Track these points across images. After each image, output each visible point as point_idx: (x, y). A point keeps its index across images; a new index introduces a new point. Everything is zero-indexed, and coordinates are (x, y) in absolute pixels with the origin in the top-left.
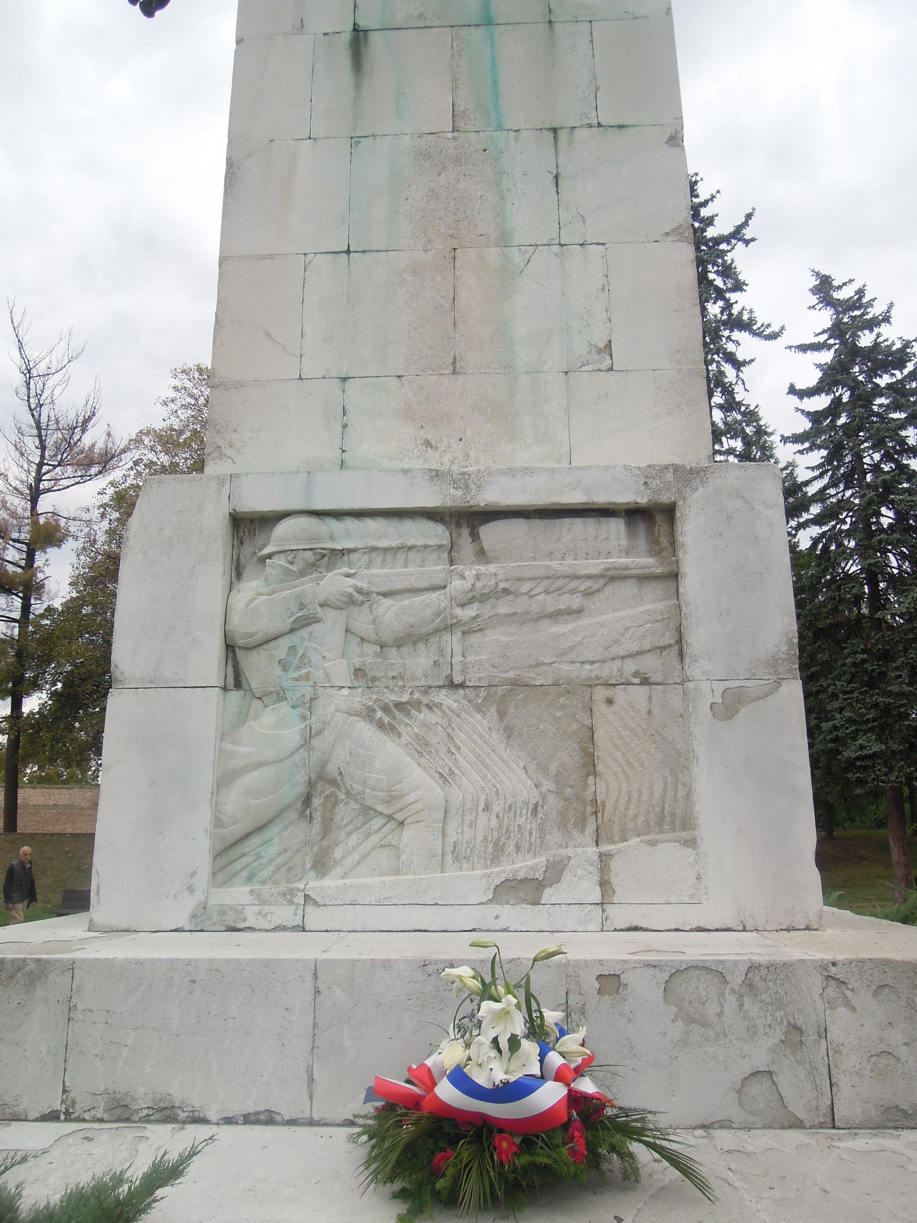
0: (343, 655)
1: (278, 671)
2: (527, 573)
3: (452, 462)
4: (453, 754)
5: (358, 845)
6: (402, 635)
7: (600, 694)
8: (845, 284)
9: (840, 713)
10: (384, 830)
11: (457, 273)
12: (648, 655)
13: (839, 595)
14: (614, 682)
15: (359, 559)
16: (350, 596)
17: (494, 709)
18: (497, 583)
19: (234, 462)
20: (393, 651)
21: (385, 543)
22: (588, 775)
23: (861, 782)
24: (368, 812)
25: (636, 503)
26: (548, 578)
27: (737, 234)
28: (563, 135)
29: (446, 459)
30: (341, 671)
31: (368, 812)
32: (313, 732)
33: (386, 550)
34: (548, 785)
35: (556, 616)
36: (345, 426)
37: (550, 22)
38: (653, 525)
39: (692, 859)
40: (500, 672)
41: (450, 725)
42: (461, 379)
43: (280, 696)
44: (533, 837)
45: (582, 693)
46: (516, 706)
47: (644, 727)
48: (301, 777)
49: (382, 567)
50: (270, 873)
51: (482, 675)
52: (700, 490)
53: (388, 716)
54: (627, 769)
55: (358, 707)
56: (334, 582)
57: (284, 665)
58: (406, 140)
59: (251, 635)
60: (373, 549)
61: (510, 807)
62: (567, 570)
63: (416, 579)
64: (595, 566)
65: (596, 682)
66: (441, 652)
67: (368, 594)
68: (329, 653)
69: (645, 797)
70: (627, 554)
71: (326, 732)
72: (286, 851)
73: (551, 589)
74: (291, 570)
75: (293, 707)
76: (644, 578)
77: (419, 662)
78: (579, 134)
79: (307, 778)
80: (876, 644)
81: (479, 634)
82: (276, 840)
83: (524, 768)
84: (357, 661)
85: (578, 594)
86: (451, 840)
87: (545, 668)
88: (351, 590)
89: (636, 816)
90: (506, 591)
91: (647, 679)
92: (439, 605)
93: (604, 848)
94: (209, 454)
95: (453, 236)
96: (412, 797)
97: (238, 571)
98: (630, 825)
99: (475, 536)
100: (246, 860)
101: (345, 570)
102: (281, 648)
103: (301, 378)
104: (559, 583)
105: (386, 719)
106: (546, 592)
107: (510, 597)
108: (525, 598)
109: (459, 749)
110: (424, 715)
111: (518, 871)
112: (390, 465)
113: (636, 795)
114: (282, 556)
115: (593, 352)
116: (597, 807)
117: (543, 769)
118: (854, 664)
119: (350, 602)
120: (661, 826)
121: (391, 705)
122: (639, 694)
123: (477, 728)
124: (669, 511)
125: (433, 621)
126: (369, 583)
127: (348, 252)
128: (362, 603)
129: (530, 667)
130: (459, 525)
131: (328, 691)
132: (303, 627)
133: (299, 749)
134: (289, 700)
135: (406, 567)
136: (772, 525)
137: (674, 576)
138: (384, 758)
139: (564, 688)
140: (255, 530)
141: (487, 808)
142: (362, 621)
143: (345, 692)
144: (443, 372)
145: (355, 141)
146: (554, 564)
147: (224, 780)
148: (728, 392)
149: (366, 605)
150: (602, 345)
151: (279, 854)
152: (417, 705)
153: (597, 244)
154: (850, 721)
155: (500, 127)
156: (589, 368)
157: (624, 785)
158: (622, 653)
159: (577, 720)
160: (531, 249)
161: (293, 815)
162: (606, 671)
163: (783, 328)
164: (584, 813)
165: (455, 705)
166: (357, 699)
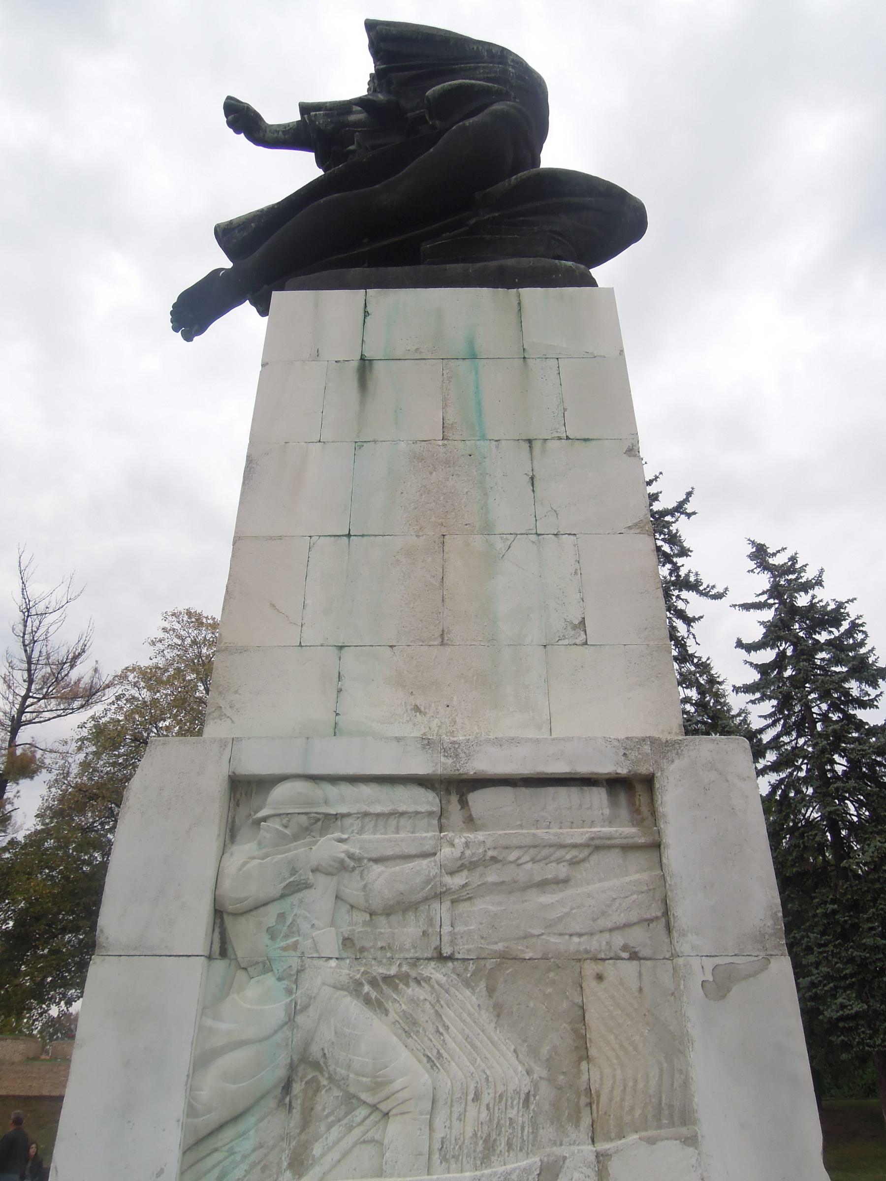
0: (333, 924)
1: (266, 940)
2: (515, 842)
3: (440, 727)
4: (441, 1034)
5: (339, 1140)
6: (391, 903)
7: (590, 968)
8: (778, 552)
9: (817, 968)
10: (368, 1122)
11: (446, 556)
12: (636, 927)
13: (803, 843)
14: (603, 956)
15: (352, 825)
16: (342, 862)
17: (482, 985)
18: (485, 851)
19: (233, 722)
20: (382, 920)
21: (378, 809)
22: (580, 1060)
23: (846, 1046)
24: (351, 1101)
25: (617, 774)
26: (535, 847)
27: (680, 508)
28: (537, 445)
29: (434, 724)
30: (328, 940)
31: (351, 1101)
32: (298, 1007)
33: (378, 815)
34: (540, 1071)
35: (543, 885)
36: (339, 691)
37: (524, 358)
38: (634, 796)
39: (694, 1161)
40: (488, 944)
41: (438, 1001)
42: (448, 650)
43: (266, 967)
44: (526, 1133)
45: (571, 968)
46: (505, 982)
47: (636, 1006)
48: (283, 1059)
49: (374, 833)
50: (243, 1173)
51: (471, 946)
52: (677, 762)
53: (375, 991)
54: (621, 1053)
55: (344, 979)
56: (327, 847)
57: (272, 934)
58: (403, 445)
59: (241, 901)
60: (366, 814)
61: (501, 1096)
62: (553, 839)
63: (407, 847)
64: (579, 835)
65: (585, 956)
66: (430, 921)
67: (358, 859)
68: (319, 923)
69: (641, 1085)
70: (611, 823)
71: (311, 1009)
72: (261, 1146)
73: (538, 857)
74: (285, 834)
75: (280, 979)
76: (627, 848)
77: (408, 931)
78: (553, 445)
79: (289, 1061)
80: (845, 894)
81: (467, 904)
82: (252, 1133)
83: (515, 1051)
84: (345, 930)
85: (565, 863)
86: (439, 1135)
87: (533, 940)
88: (343, 855)
89: (632, 1109)
90: (494, 860)
91: (636, 953)
92: (429, 872)
93: (603, 1146)
94: (210, 714)
95: (442, 524)
96: (397, 1085)
97: (232, 833)
98: (627, 1119)
99: (463, 803)
100: (218, 1156)
101: (338, 835)
102: (270, 915)
103: (300, 645)
104: (546, 852)
105: (374, 994)
106: (533, 860)
107: (499, 866)
108: (513, 866)
109: (447, 1028)
110: (413, 990)
111: (510, 1174)
113: (631, 1084)
114: (277, 819)
115: (569, 628)
116: (591, 1097)
117: (534, 1052)
118: (825, 915)
119: (341, 868)
120: (659, 1120)
121: (379, 979)
122: (629, 969)
123: (465, 1006)
124: (649, 782)
125: (423, 889)
126: (360, 848)
127: (349, 535)
128: (354, 869)
129: (518, 938)
130: (448, 792)
131: (315, 962)
132: (293, 893)
133: (282, 1026)
134: (276, 971)
135: (397, 833)
136: (747, 797)
137: (656, 846)
138: (369, 1038)
139: (553, 962)
140: (252, 792)
141: (477, 1098)
142: (352, 888)
143: (333, 963)
144: (431, 643)
145: (359, 445)
146: (540, 832)
147: (202, 1061)
148: (680, 644)
149: (357, 871)
150: (576, 622)
151: (254, 1150)
152: (405, 978)
153: (569, 534)
154: (828, 977)
155: (483, 438)
156: (566, 642)
157: (619, 1072)
158: (610, 925)
159: (567, 998)
160: (511, 537)
161: (271, 1103)
162: (595, 944)
163: (726, 589)
164: (577, 1104)
165: (443, 980)
166: (344, 971)
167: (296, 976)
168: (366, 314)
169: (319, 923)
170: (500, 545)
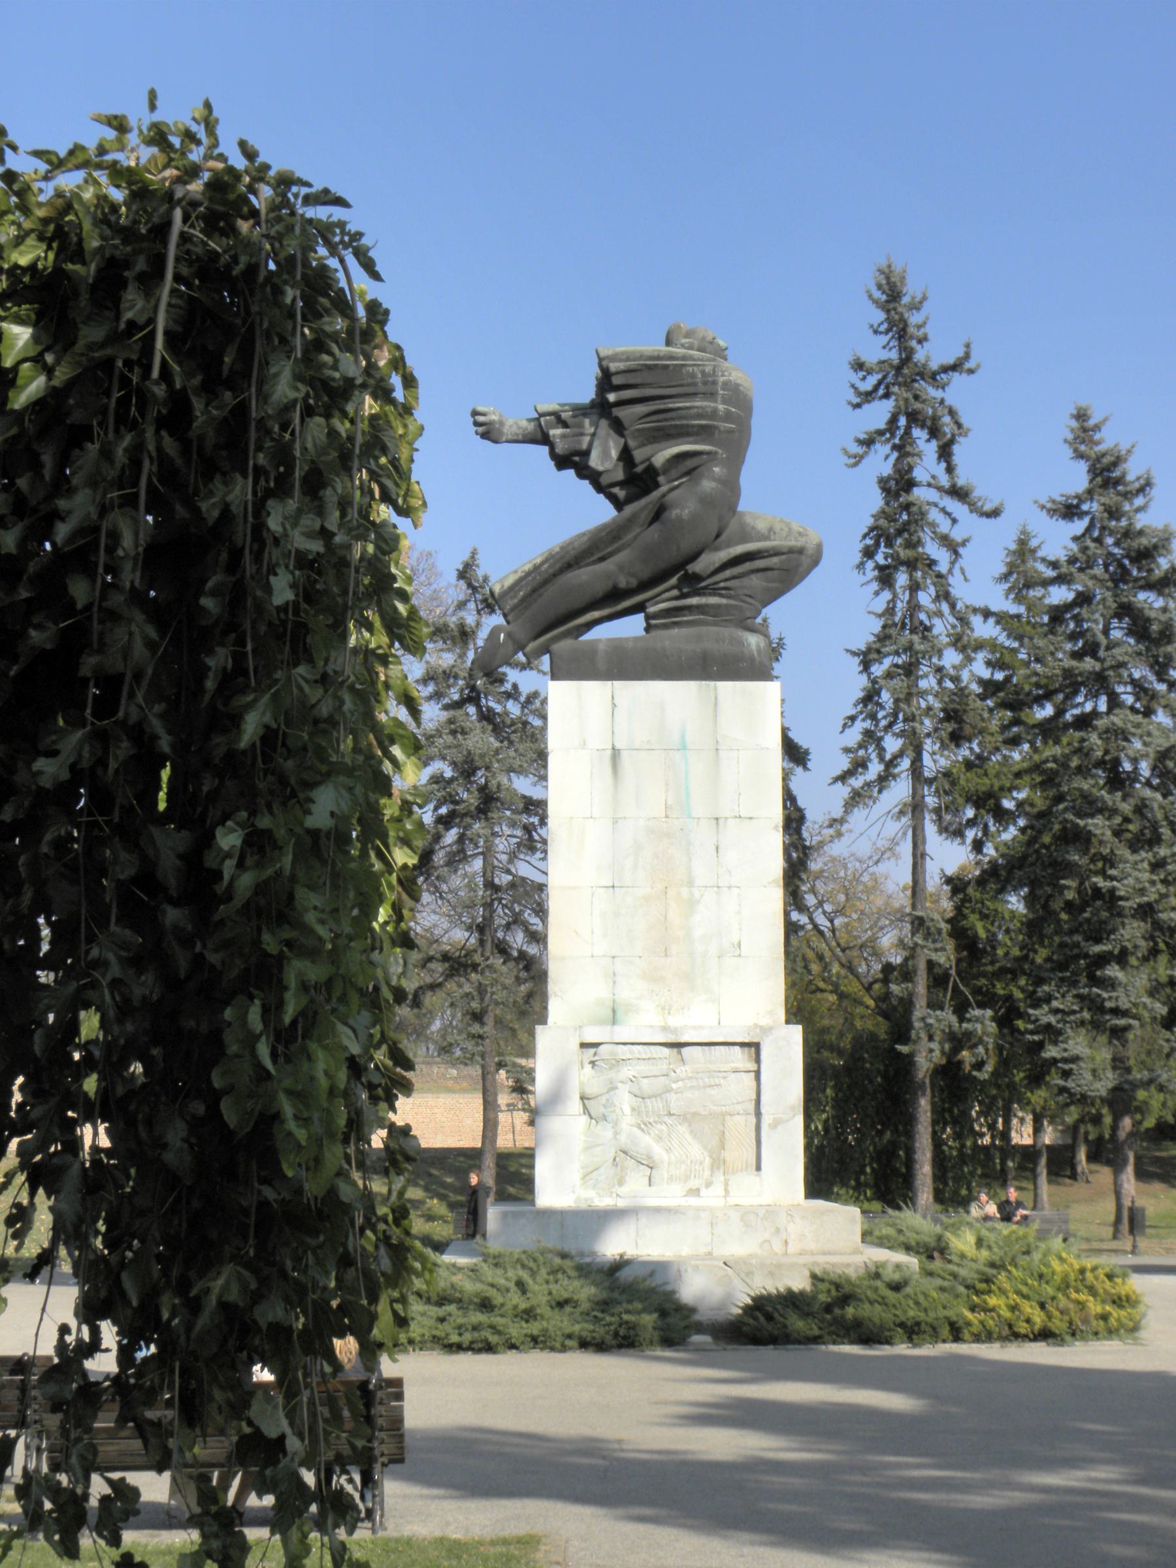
28: (721, 821)
30: (627, 1110)
57: (605, 1106)
68: (624, 1101)
77: (658, 1105)
78: (731, 822)
112: (645, 1023)
117: (705, 1148)
138: (647, 1142)
145: (615, 821)
155: (690, 817)
167: (616, 1123)
168: (614, 705)
169: (624, 1101)
170: (697, 894)
